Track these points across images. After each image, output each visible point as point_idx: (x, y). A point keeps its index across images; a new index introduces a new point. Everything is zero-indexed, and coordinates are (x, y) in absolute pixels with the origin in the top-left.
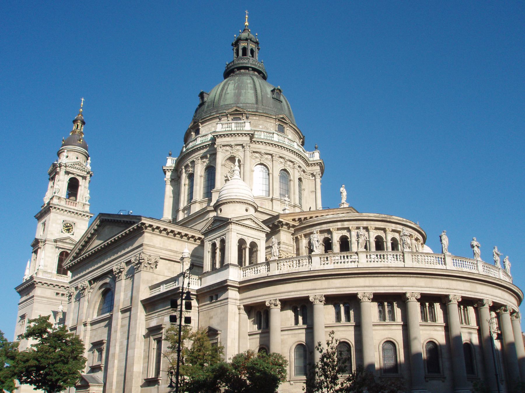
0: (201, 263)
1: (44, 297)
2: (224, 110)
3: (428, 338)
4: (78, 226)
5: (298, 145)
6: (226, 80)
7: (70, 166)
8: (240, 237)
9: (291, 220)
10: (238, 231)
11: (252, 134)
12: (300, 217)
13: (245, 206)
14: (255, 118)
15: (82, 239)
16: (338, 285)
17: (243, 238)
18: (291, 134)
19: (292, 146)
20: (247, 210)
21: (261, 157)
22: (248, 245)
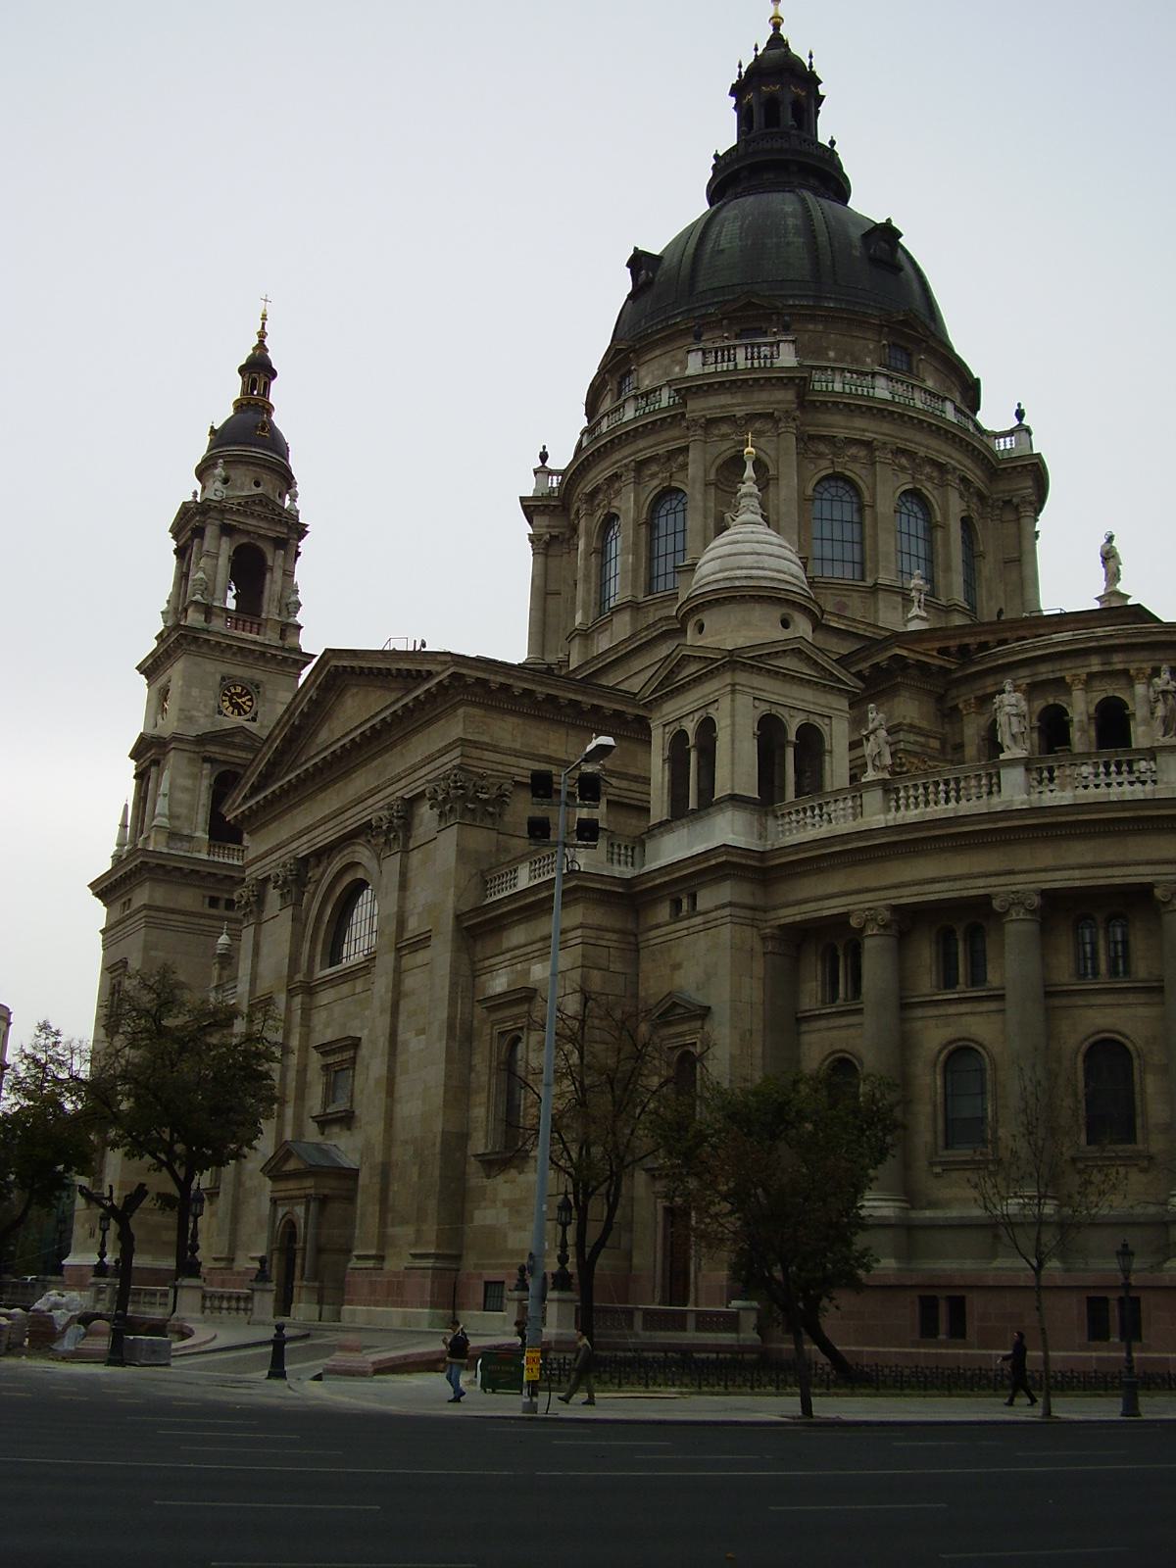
0: (644, 797)
2: (709, 305)
4: (269, 694)
5: (957, 409)
6: (714, 208)
7: (235, 507)
8: (764, 708)
9: (935, 653)
11: (802, 378)
12: (967, 640)
13: (776, 613)
14: (811, 327)
15: (277, 732)
16: (1089, 859)
17: (773, 712)
19: (939, 413)
20: (785, 624)
21: (834, 454)
22: (792, 736)
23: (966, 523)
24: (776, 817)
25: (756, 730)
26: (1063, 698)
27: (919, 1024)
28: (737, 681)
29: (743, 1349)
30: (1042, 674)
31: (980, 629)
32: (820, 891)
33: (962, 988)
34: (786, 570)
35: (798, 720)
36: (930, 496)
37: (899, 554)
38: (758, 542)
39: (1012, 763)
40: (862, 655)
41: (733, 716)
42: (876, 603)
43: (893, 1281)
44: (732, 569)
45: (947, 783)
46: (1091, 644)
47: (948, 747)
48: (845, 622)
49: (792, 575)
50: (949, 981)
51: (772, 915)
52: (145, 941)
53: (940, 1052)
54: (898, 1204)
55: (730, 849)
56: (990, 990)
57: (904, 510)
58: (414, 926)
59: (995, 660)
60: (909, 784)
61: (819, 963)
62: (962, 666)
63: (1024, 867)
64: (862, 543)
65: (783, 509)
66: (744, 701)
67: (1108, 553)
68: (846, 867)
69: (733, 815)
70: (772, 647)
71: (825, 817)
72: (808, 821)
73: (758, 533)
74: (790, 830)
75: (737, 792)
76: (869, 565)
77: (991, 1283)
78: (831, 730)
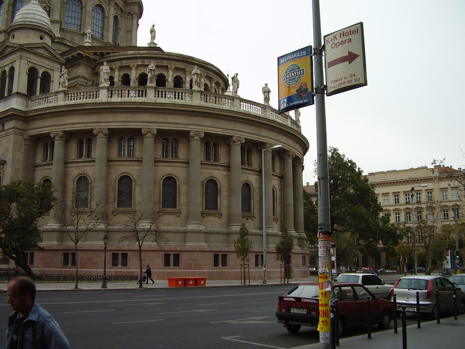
3: (209, 176)
9: (92, 54)
10: (30, 59)
12: (103, 51)
13: (39, 34)
16: (123, 120)
17: (34, 66)
20: (41, 38)
22: (40, 75)
23: (116, 18)
24: (32, 101)
25: (27, 72)
26: (129, 72)
27: (70, 169)
28: (22, 55)
29: (10, 270)
30: (124, 63)
31: (108, 48)
32: (43, 125)
33: (84, 158)
34: (43, 21)
35: (42, 70)
36: (105, 8)
37: (93, 25)
38: (35, 10)
39: (103, 88)
40: (69, 52)
41: (20, 66)
42: (83, 39)
43: (55, 248)
44: (25, 18)
45: (84, 92)
46: (139, 56)
47: (95, 85)
48: (72, 44)
49: (45, 23)
50: (81, 156)
51: (28, 132)
54: (59, 224)
55: (14, 110)
56: (92, 159)
57: (96, 10)
59: (110, 58)
60: (72, 92)
61: (42, 148)
62: (100, 59)
63: (104, 121)
64: (81, 19)
65: (55, 5)
66: (24, 62)
67: (152, 30)
68: (51, 118)
69: (17, 99)
70: (35, 45)
71: (46, 101)
72: (41, 102)
73: (36, 7)
74: (36, 105)
75: (19, 91)
76: (82, 27)
77: (84, 249)
78: (54, 74)
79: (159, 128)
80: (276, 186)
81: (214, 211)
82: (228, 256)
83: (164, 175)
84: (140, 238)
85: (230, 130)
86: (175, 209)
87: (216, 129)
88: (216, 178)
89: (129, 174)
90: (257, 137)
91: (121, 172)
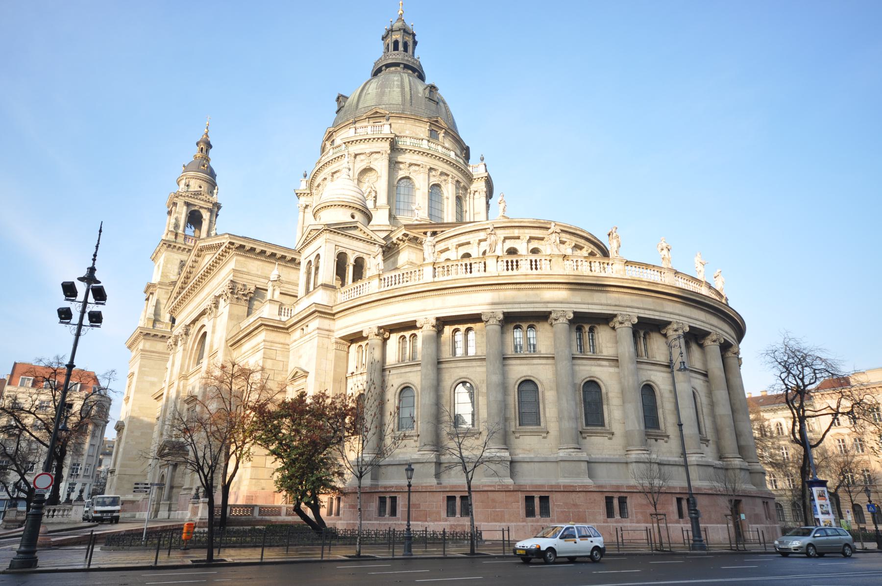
1: (153, 352)
3: (587, 376)
5: (456, 155)
7: (190, 195)
8: (341, 249)
9: (422, 234)
13: (350, 212)
14: (400, 121)
17: (344, 251)
18: (450, 143)
20: (353, 217)
49: (358, 198)
52: (140, 364)
53: (398, 389)
58: (215, 348)
79: (505, 310)
80: (698, 389)
81: (600, 428)
82: (628, 501)
83: (519, 377)
84: (468, 470)
85: (613, 306)
86: (538, 427)
87: (590, 306)
88: (599, 379)
89: (468, 378)
90: (658, 314)
91: (459, 377)
